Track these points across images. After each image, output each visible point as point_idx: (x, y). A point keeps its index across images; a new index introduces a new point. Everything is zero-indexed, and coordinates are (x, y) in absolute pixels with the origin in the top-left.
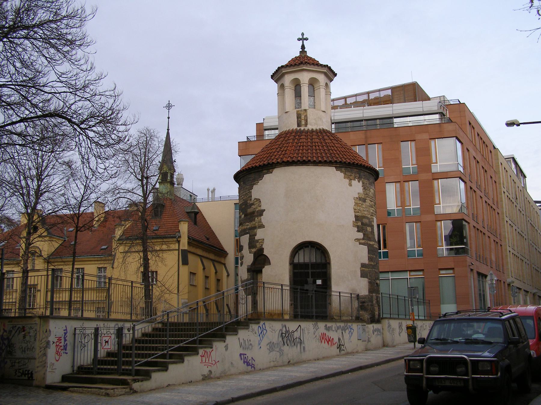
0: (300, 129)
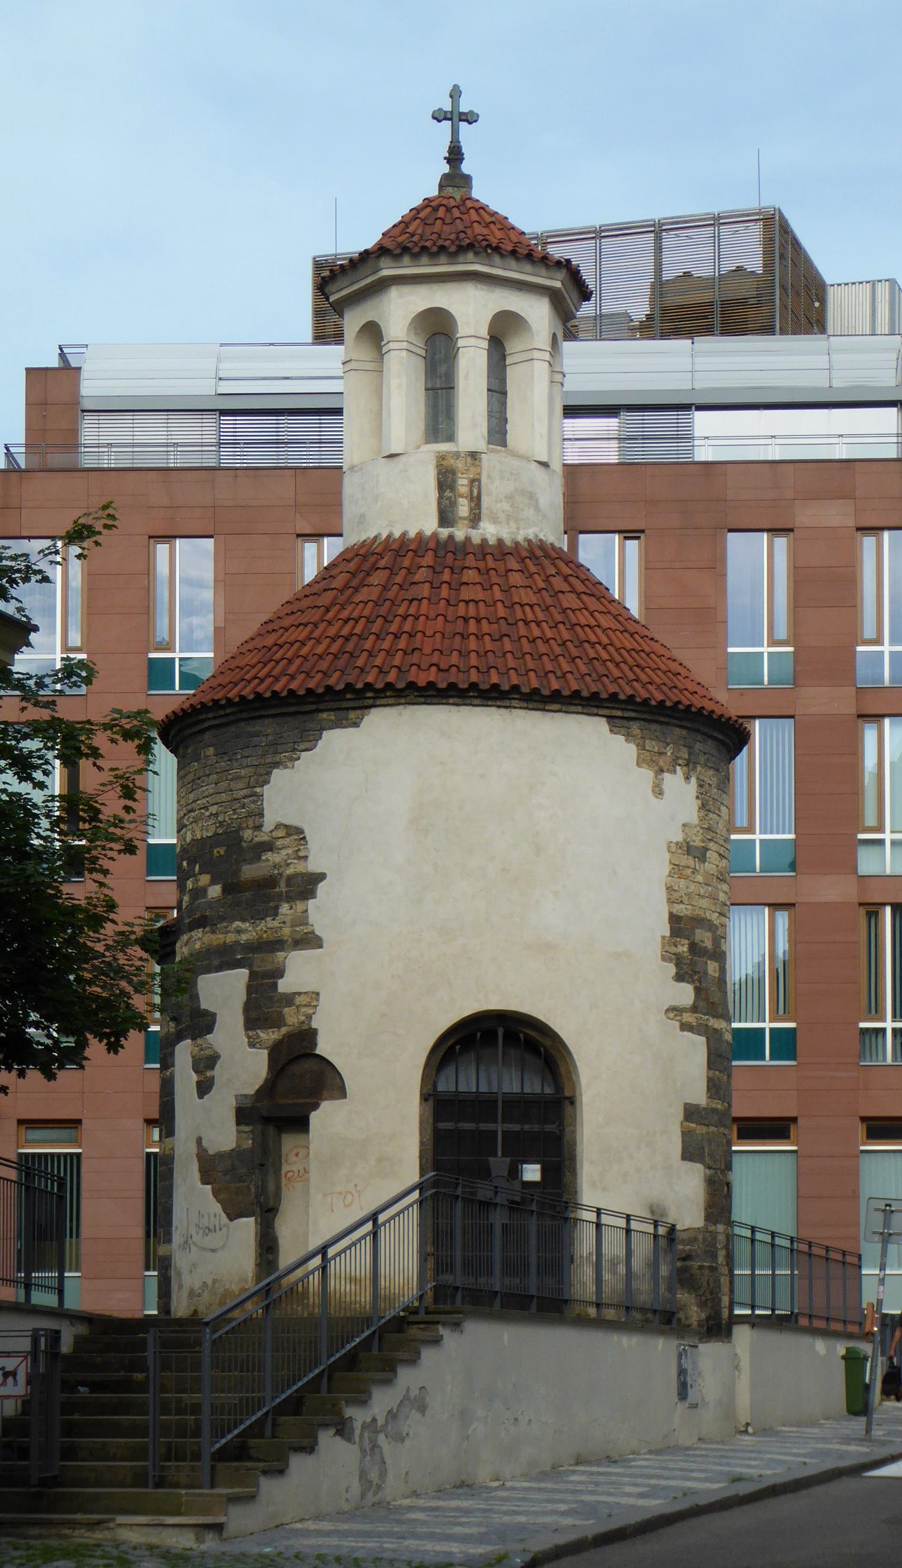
0: (451, 537)
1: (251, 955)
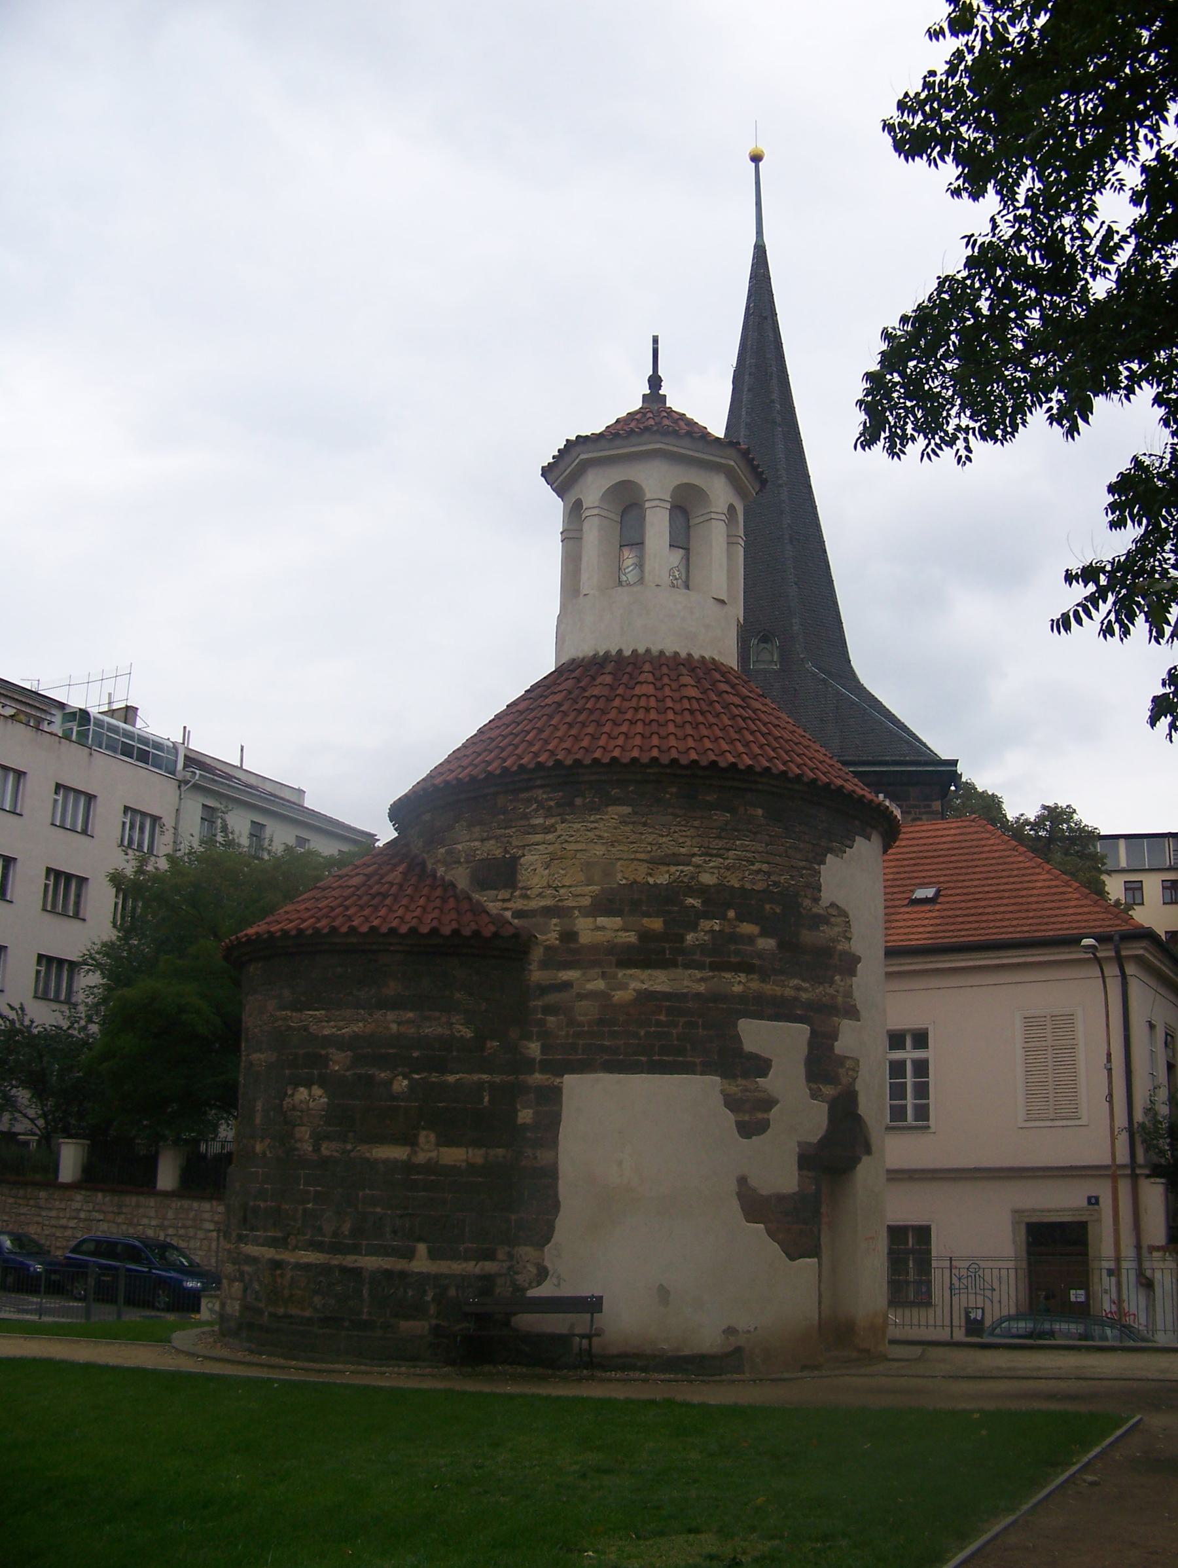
1: (812, 1014)
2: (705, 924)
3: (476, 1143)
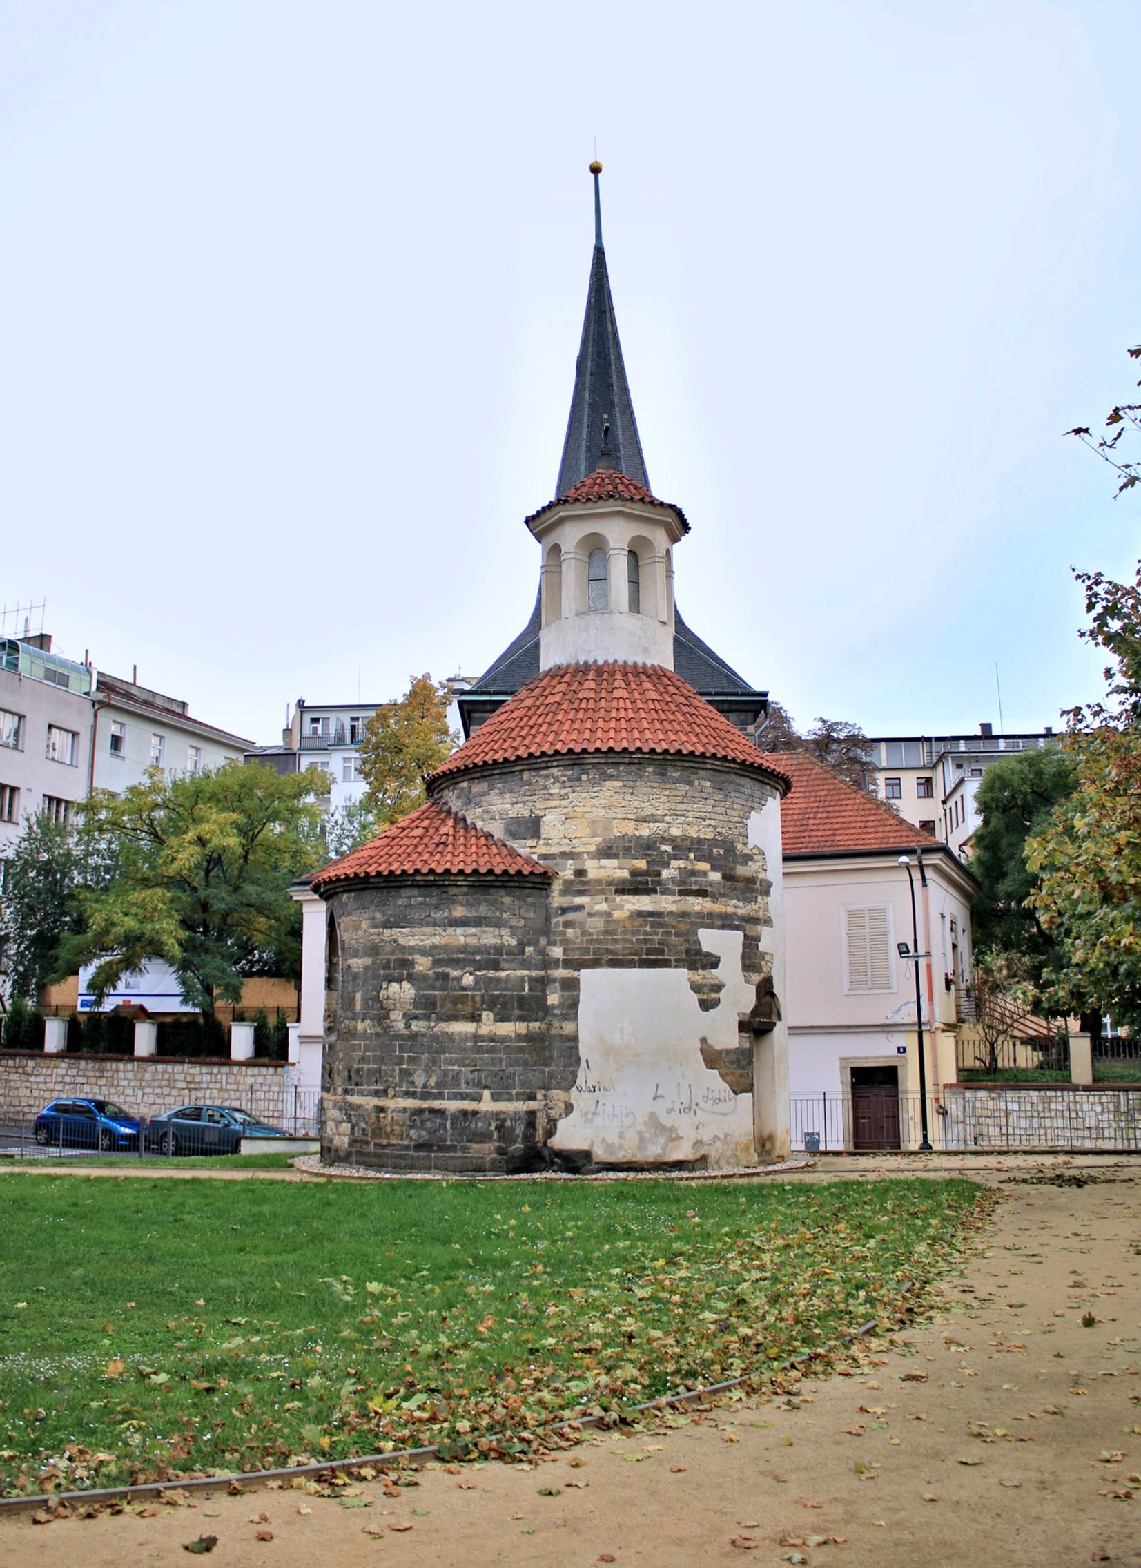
2: (674, 863)
3: (521, 1019)
